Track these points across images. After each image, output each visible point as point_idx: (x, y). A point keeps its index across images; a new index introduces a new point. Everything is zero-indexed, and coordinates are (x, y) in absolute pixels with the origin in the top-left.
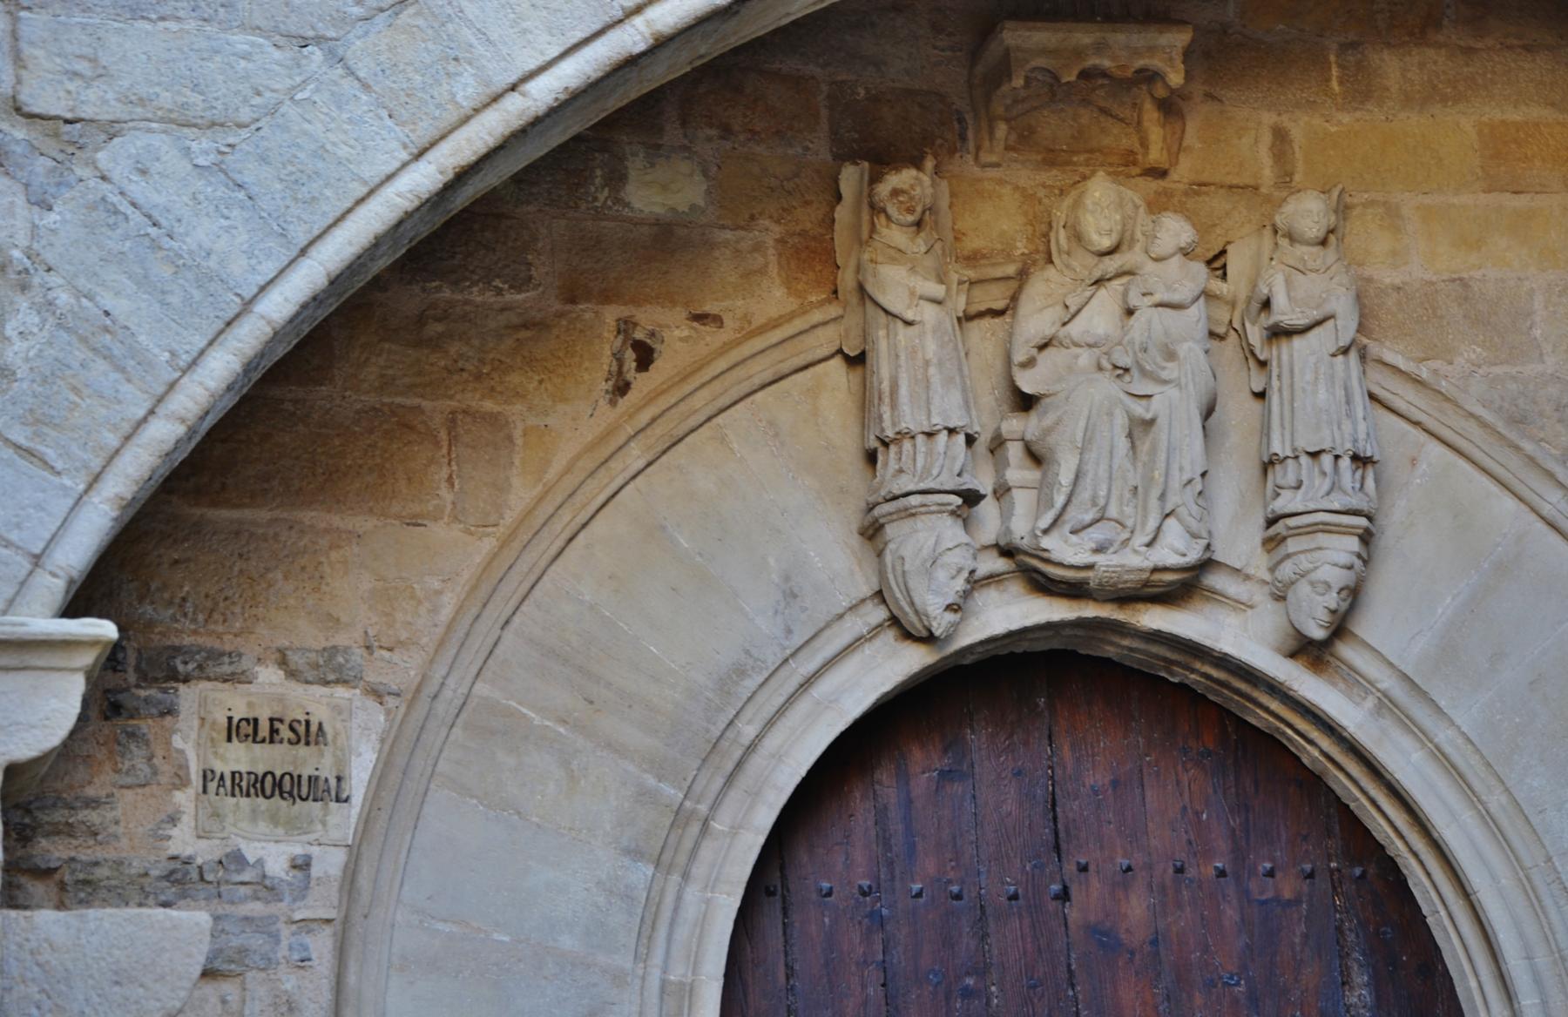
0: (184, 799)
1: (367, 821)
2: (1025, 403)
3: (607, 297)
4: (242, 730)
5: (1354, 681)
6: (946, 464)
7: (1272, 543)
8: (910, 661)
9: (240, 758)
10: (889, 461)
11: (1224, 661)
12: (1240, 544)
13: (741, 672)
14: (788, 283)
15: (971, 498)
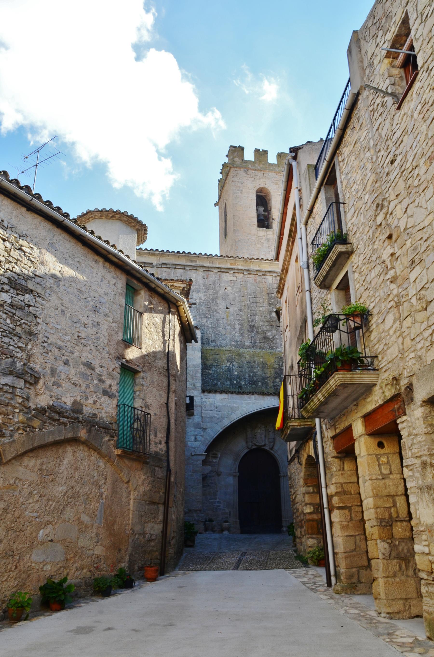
12: (267, 443)
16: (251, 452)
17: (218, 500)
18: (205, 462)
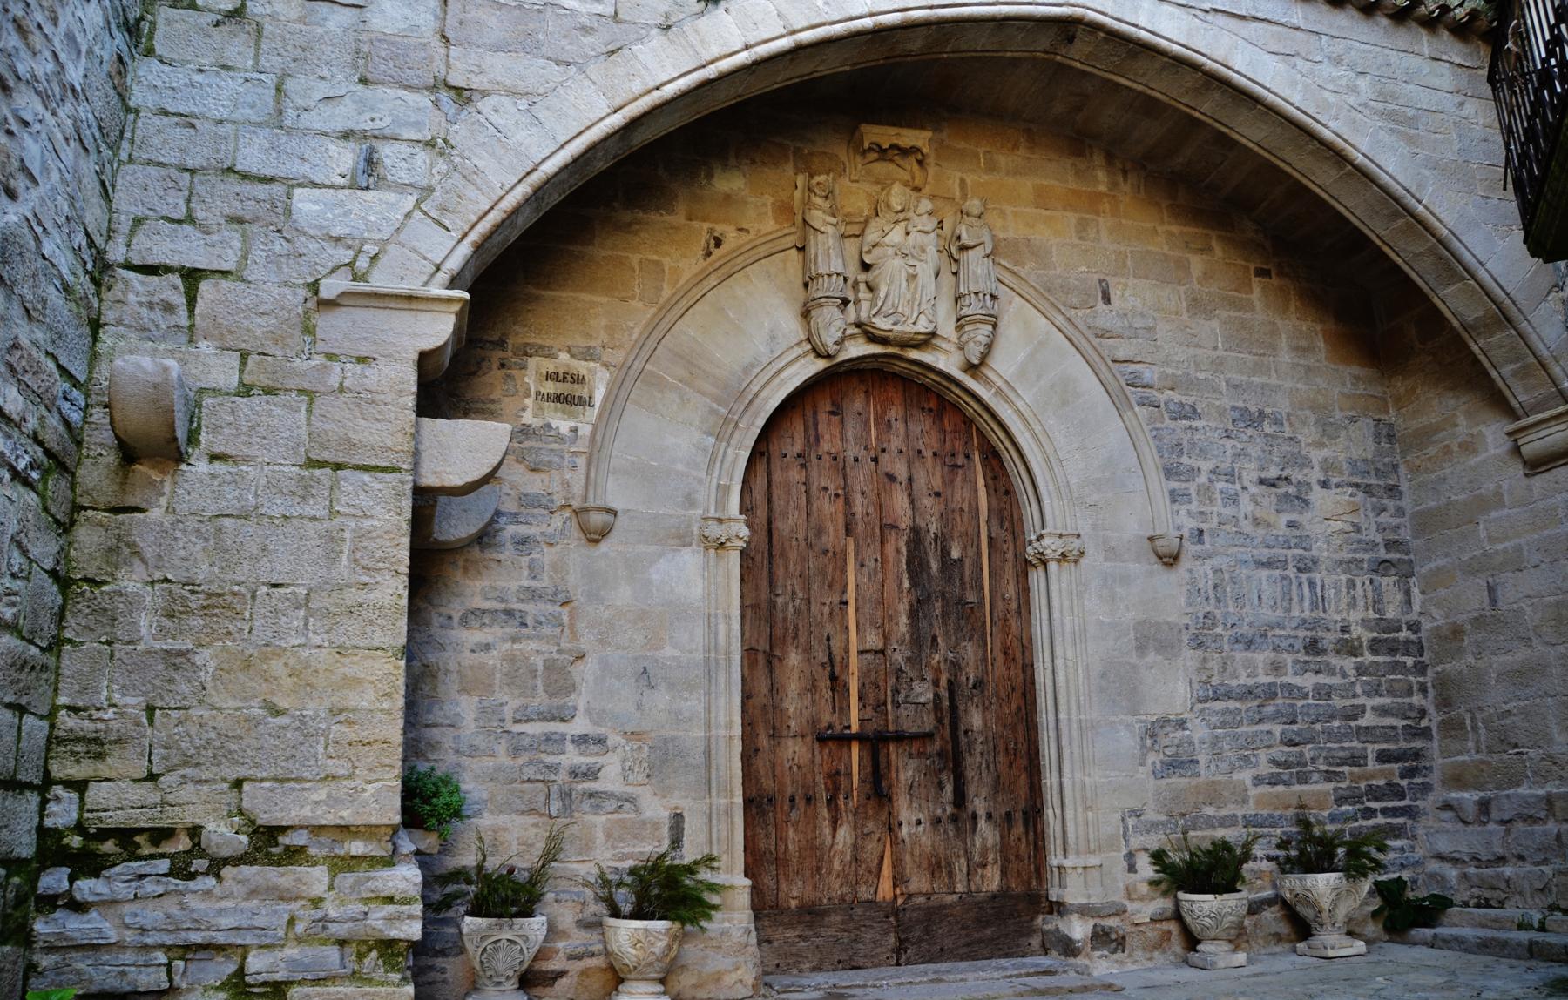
0: (529, 402)
1: (600, 414)
2: (866, 267)
3: (704, 220)
4: (553, 377)
5: (987, 382)
6: (835, 287)
7: (959, 328)
8: (821, 364)
9: (550, 387)
10: (813, 286)
11: (940, 373)
12: (947, 329)
13: (753, 366)
14: (776, 220)
15: (845, 302)
16: (832, 384)
17: (579, 726)
18: (445, 387)
